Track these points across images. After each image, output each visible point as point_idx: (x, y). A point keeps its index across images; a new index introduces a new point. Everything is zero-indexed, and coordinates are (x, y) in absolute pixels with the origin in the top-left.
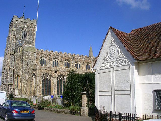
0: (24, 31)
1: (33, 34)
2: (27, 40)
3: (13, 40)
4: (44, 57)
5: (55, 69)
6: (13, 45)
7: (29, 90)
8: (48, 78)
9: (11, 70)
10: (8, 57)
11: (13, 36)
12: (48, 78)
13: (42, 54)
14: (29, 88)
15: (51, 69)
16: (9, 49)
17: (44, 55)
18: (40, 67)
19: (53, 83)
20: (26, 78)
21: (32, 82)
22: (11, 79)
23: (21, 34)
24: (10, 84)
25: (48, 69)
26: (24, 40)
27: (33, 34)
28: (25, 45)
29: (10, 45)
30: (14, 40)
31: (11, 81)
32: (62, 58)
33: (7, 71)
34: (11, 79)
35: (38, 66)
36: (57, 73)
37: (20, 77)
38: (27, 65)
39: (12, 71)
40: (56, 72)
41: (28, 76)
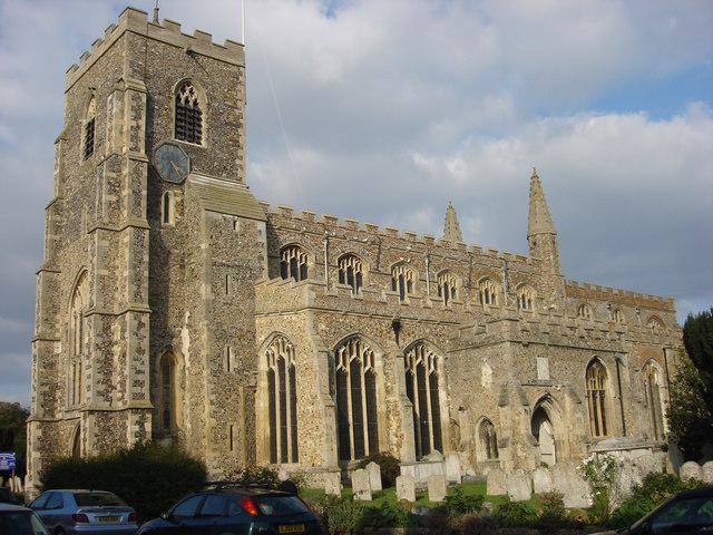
0: (183, 97)
1: (231, 118)
2: (203, 150)
3: (132, 145)
6: (136, 171)
7: (242, 437)
10: (107, 243)
11: (134, 123)
12: (362, 360)
14: (239, 427)
15: (372, 310)
16: (113, 198)
19: (388, 392)
20: (225, 366)
21: (254, 389)
22: (139, 372)
23: (173, 115)
24: (138, 403)
25: (358, 307)
26: (189, 150)
28: (198, 180)
29: (114, 175)
30: (142, 145)
33: (106, 329)
34: (140, 377)
35: (314, 294)
37: (180, 360)
38: (223, 289)
39: (141, 325)
40: (397, 326)
41: (231, 356)
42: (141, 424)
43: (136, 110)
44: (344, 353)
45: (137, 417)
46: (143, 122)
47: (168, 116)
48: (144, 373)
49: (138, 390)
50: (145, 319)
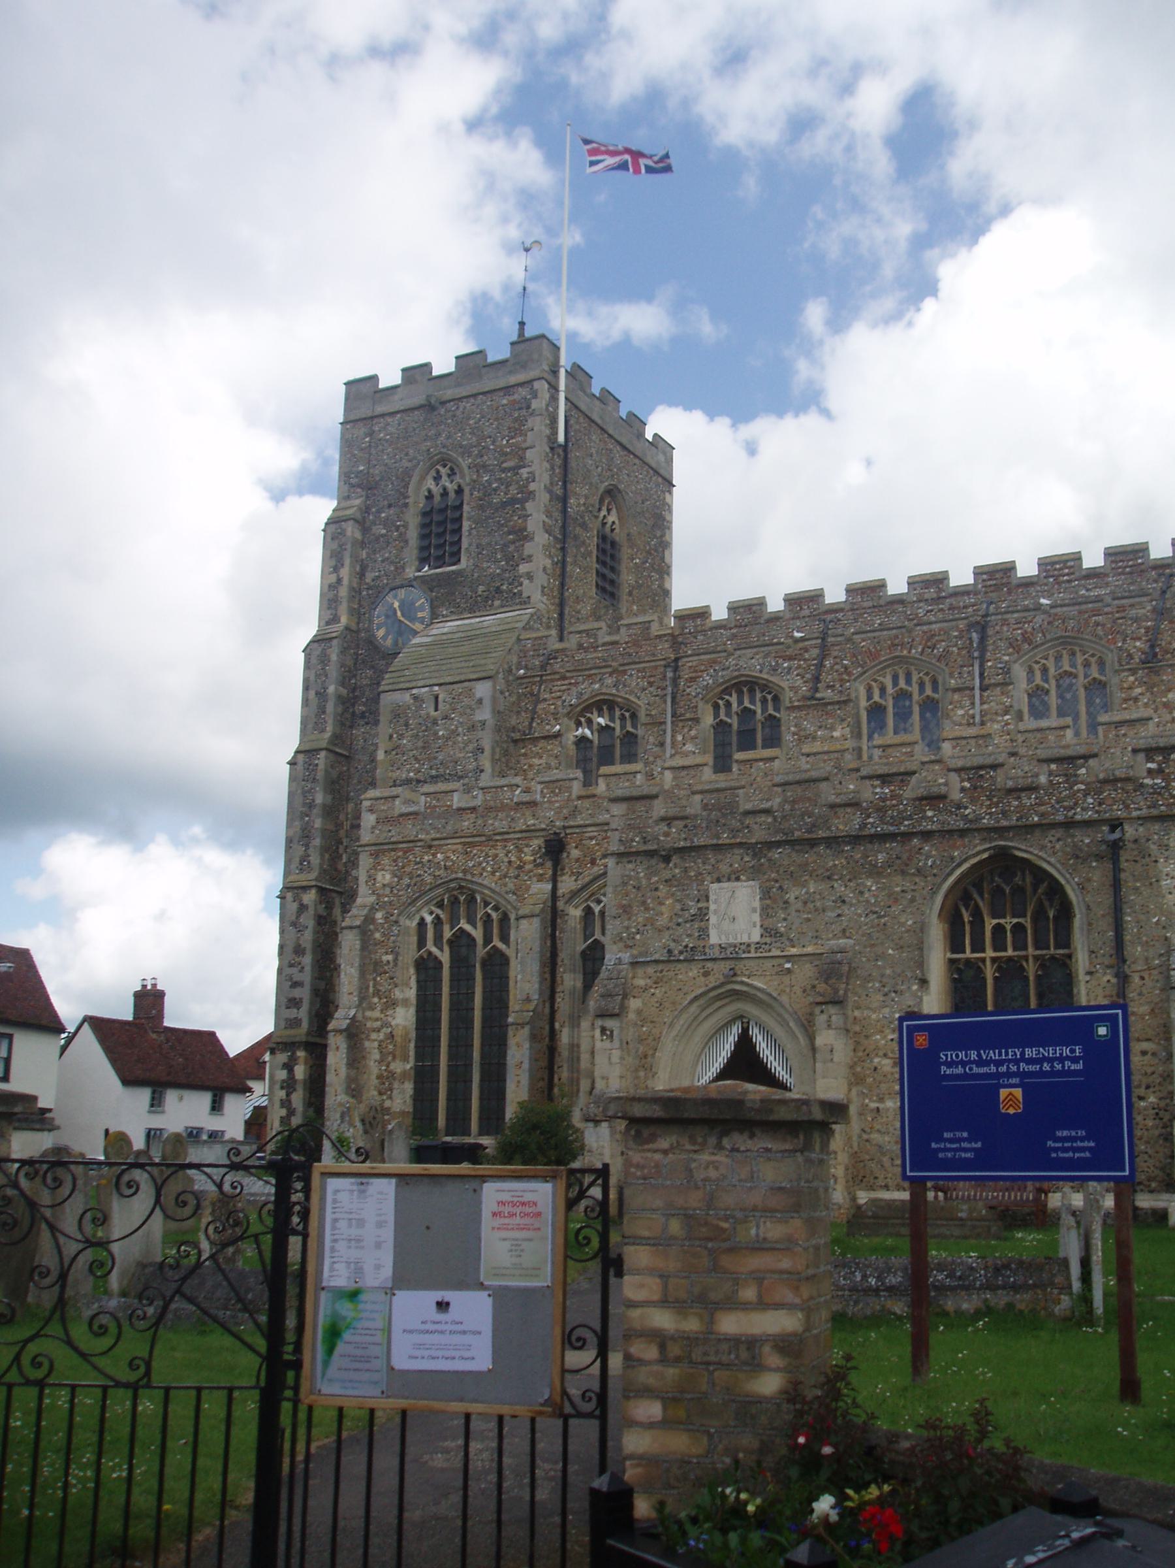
8: (477, 934)
9: (295, 906)
27: (513, 490)
32: (823, 657)
34: (297, 993)
39: (303, 908)
40: (555, 849)
42: (289, 1067)
44: (438, 922)
45: (282, 1057)
49: (293, 1013)
50: (310, 897)
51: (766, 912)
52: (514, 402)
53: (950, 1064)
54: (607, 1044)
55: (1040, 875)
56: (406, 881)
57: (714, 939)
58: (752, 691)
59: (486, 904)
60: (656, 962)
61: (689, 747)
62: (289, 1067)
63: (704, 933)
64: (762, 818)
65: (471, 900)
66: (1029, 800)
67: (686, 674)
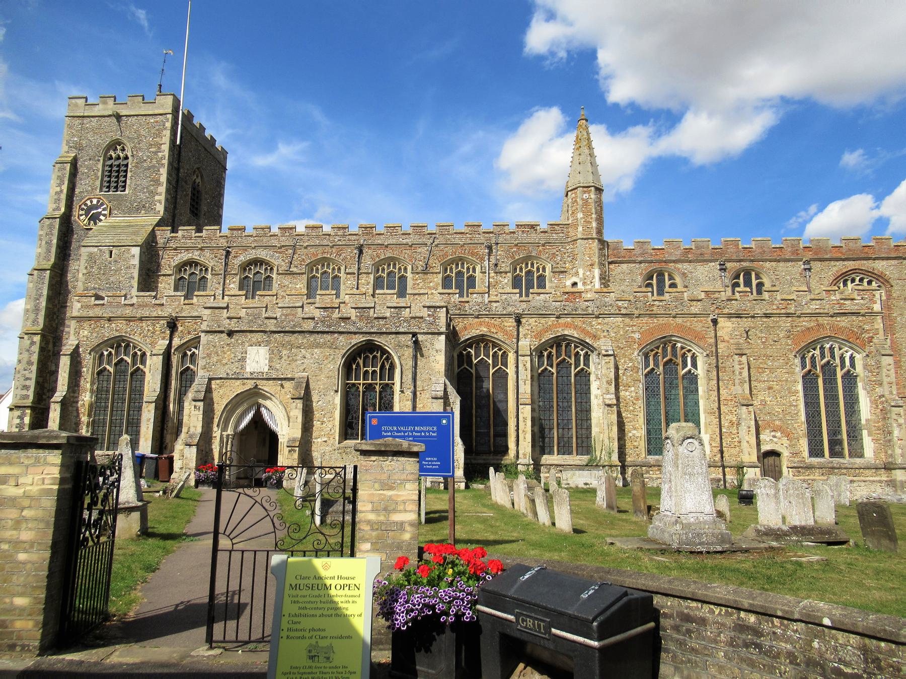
3: (54, 206)
4: (197, 264)
5: (168, 311)
8: (129, 360)
9: (29, 342)
11: (58, 189)
13: (187, 249)
17: (197, 253)
18: (88, 307)
22: (27, 379)
23: (100, 174)
25: (128, 312)
27: (154, 161)
31: (26, 387)
34: (28, 383)
35: (79, 305)
36: (180, 329)
39: (33, 343)
40: (173, 326)
42: (21, 418)
43: (61, 179)
46: (65, 188)
47: (96, 174)
48: (30, 379)
49: (25, 392)
50: (37, 339)
51: (271, 360)
52: (157, 122)
53: (385, 432)
54: (197, 412)
55: (384, 352)
56: (95, 335)
57: (248, 370)
58: (261, 264)
59: (135, 347)
60: (221, 378)
61: (232, 286)
62: (21, 418)
63: (243, 367)
64: (272, 321)
65: (127, 346)
66: (382, 322)
67: (232, 255)
